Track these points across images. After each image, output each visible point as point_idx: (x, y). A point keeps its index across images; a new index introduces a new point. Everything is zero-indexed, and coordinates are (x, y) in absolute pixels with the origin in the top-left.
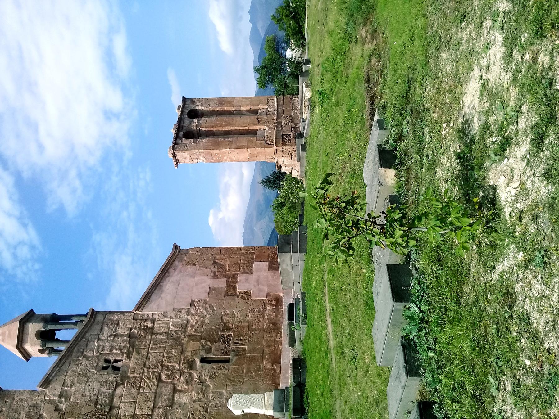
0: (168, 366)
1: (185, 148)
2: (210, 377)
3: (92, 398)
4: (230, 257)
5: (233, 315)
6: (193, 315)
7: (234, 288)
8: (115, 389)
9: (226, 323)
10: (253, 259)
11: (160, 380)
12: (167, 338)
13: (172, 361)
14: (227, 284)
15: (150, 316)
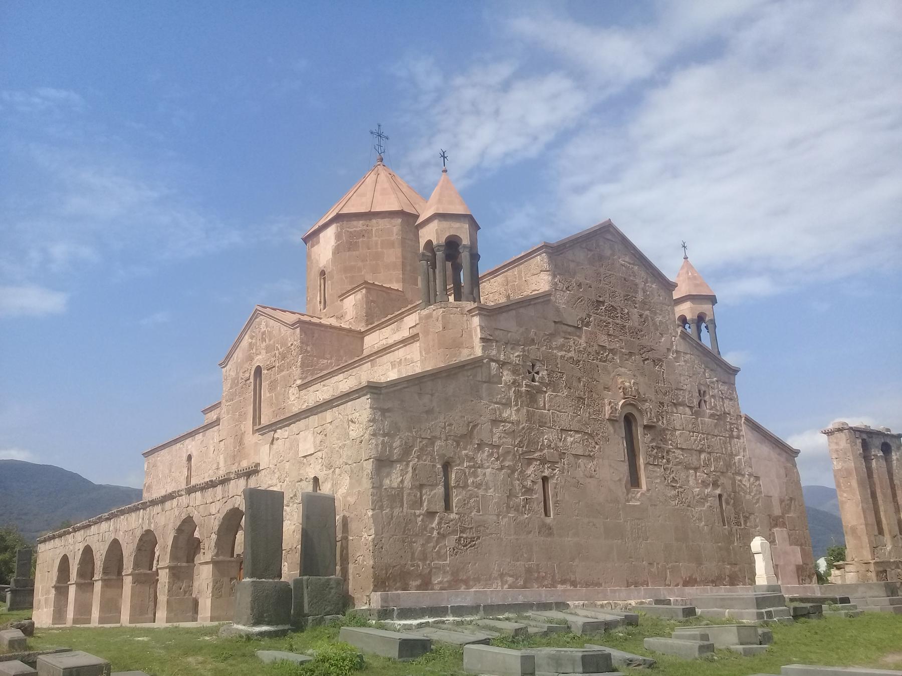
0: (710, 459)
1: (853, 443)
2: (711, 506)
3: (680, 384)
4: (798, 517)
5: (756, 526)
6: (749, 480)
7: (776, 525)
8: (688, 406)
9: (749, 519)
10: (801, 545)
11: (701, 451)
12: (729, 455)
13: (715, 463)
14: (778, 516)
15: (741, 433)
